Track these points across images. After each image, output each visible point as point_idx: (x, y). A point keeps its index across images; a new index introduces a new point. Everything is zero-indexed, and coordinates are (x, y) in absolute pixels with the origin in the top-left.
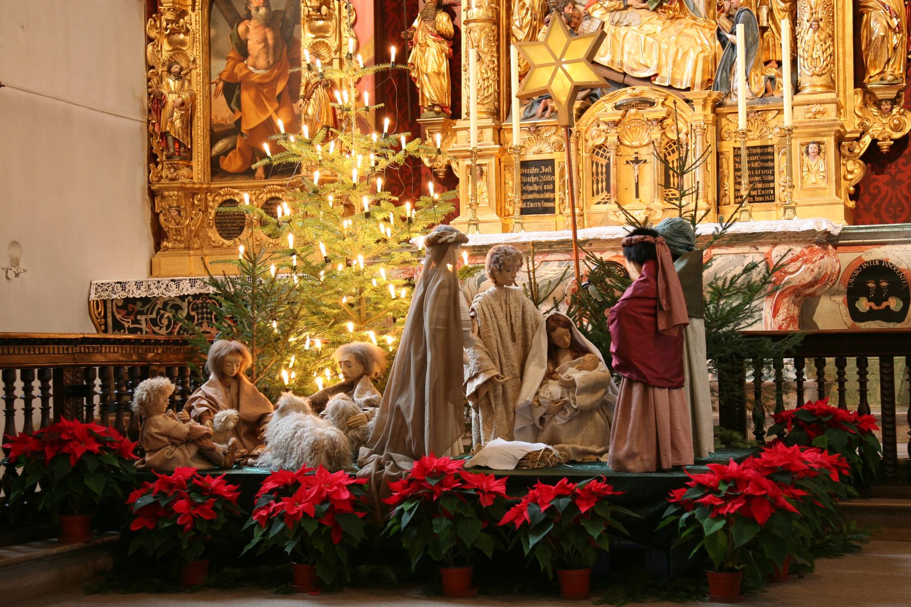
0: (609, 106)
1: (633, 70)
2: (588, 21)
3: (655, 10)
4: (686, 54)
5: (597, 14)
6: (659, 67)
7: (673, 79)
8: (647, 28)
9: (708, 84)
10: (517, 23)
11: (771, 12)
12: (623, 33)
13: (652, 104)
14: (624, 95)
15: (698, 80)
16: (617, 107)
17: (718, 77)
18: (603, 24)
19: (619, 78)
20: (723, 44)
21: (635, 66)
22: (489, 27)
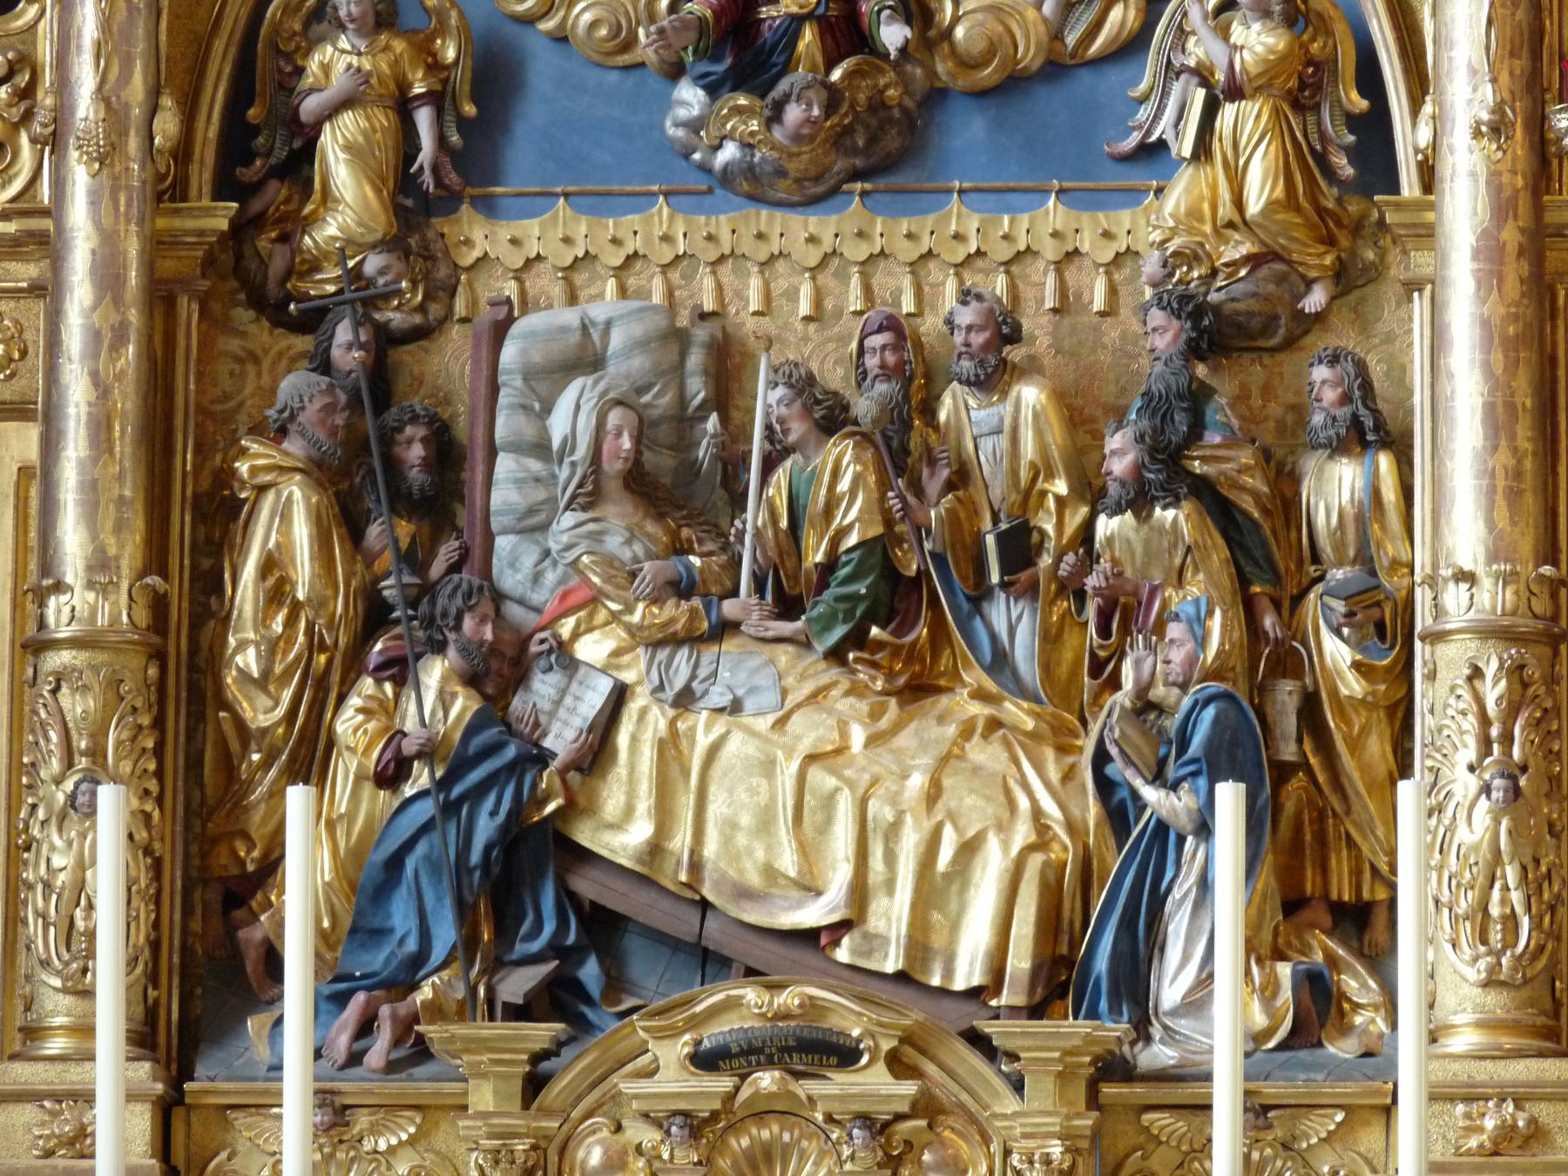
0: (672, 1053)
1: (744, 894)
2: (555, 678)
3: (836, 655)
4: (969, 849)
5: (592, 649)
6: (859, 893)
7: (919, 947)
8: (809, 731)
9: (1057, 983)
10: (249, 660)
11: (1310, 708)
12: (703, 741)
13: (846, 1055)
14: (747, 1007)
15: (1020, 961)
16: (706, 1060)
17: (1095, 952)
18: (620, 695)
19: (684, 924)
20: (1119, 811)
21: (754, 879)
22: (136, 670)
